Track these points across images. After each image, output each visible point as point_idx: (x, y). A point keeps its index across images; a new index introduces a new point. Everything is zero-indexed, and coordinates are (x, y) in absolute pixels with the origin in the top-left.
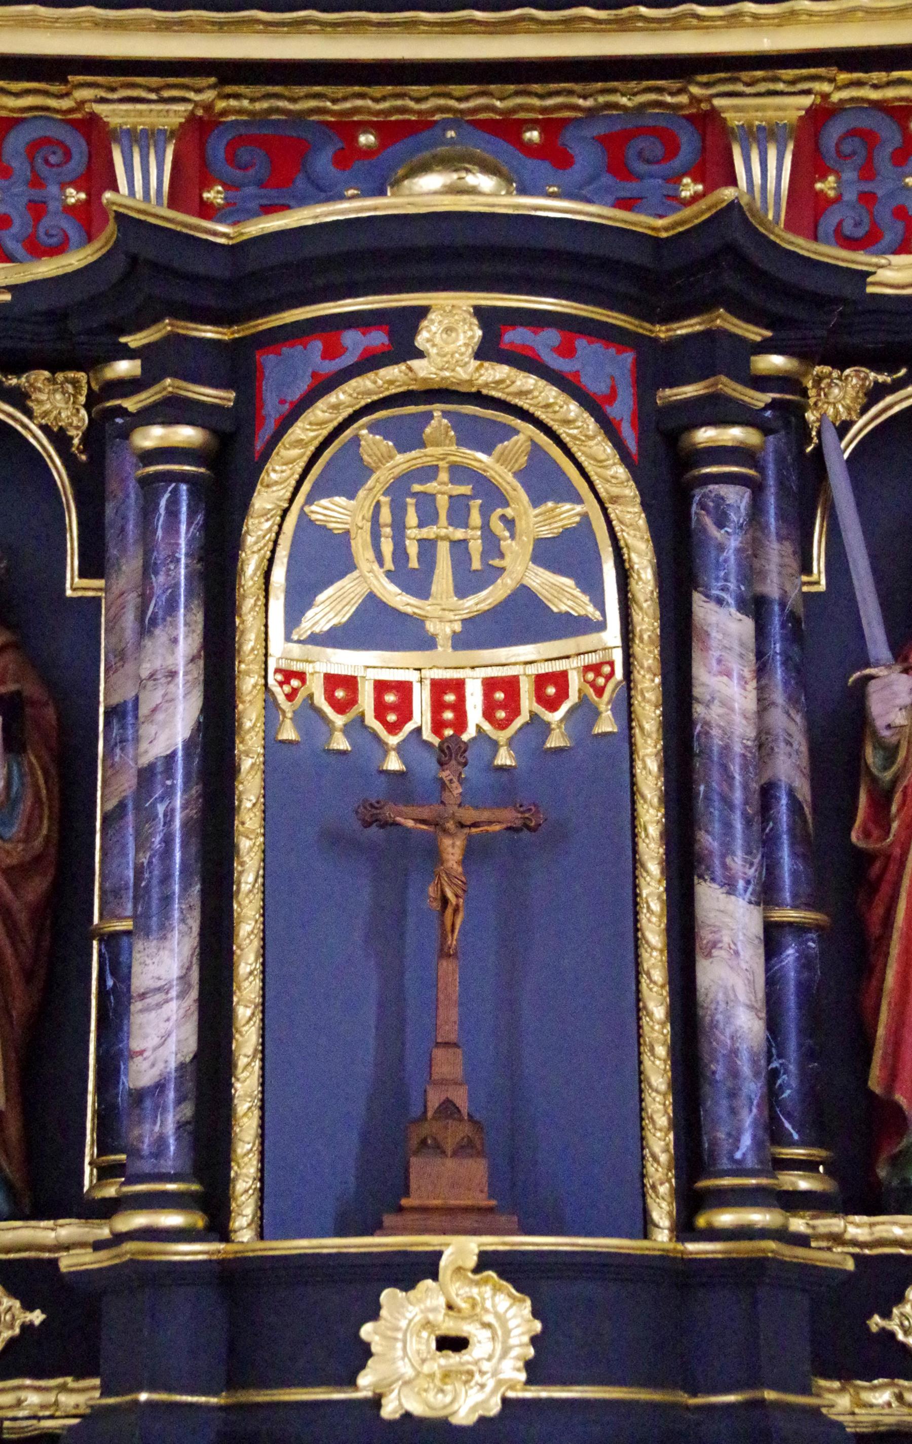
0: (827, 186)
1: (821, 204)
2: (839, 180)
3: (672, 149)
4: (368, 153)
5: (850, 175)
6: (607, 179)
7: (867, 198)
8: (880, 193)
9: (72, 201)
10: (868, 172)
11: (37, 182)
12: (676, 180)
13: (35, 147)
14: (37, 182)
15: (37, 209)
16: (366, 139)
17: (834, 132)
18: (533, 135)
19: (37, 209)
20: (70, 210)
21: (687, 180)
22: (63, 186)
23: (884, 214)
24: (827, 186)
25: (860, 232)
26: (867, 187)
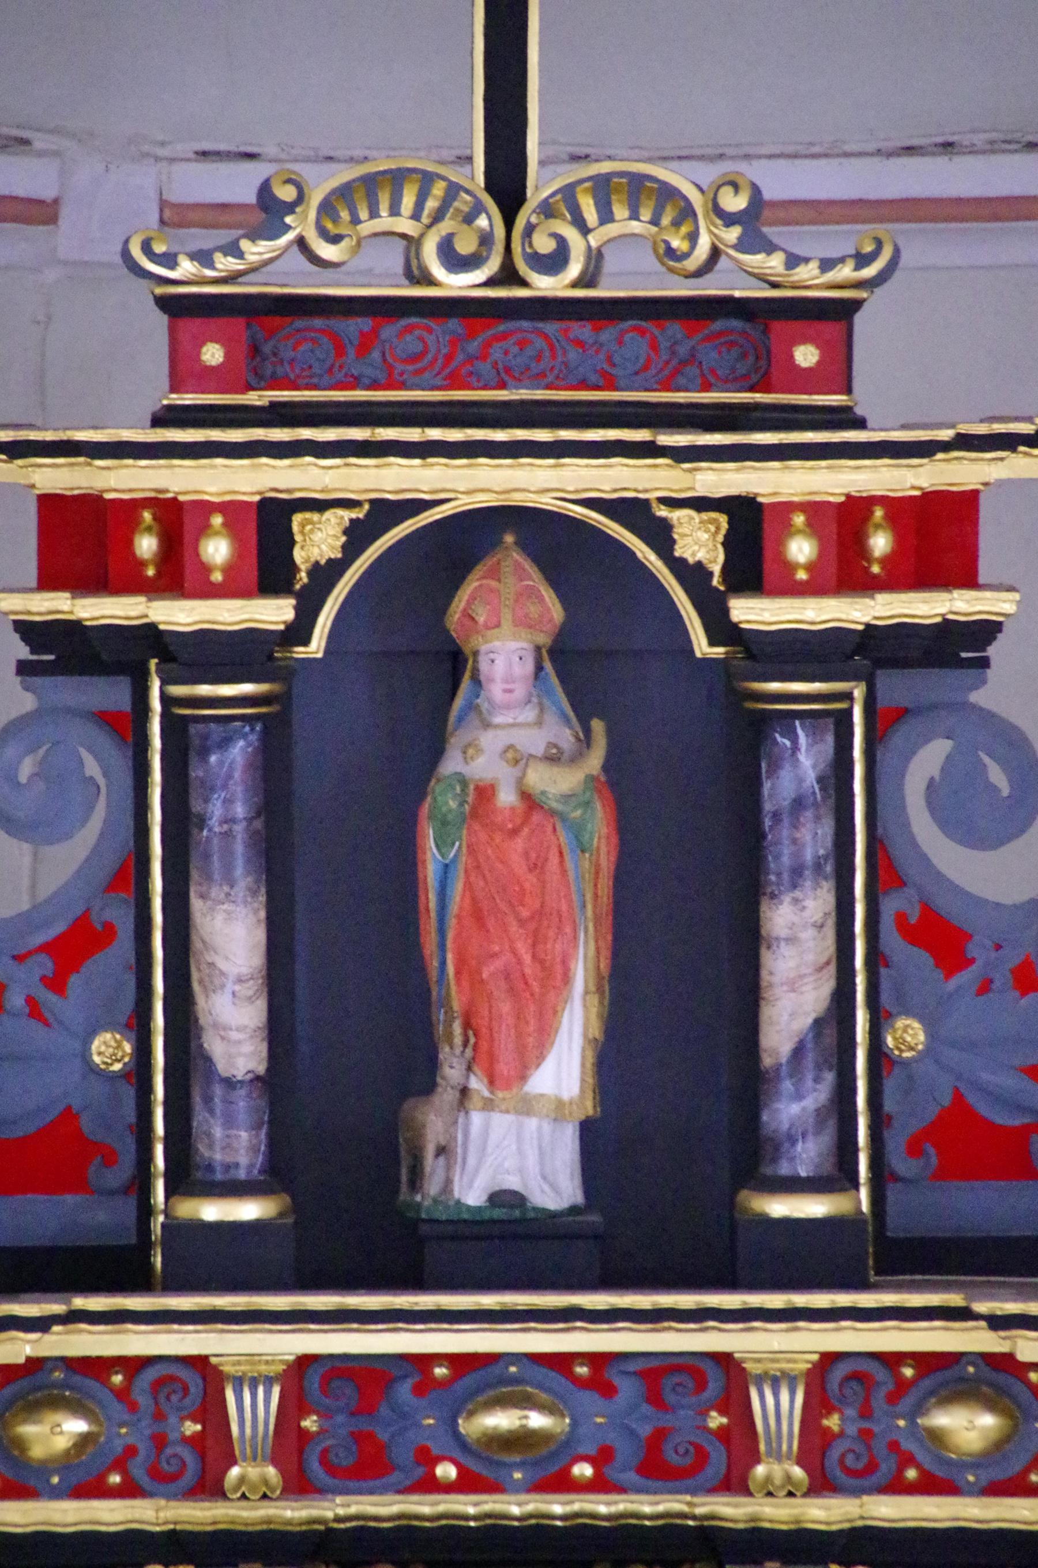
0: (833, 1422)
1: (828, 1438)
2: (842, 1419)
3: (701, 1385)
4: (443, 1384)
5: (851, 1412)
6: (646, 1409)
7: (866, 1435)
8: (876, 1429)
9: (188, 1433)
10: (866, 1412)
11: (159, 1416)
12: (704, 1413)
13: (158, 1385)
14: (159, 1416)
15: (159, 1441)
16: (440, 1371)
17: (840, 1371)
18: (582, 1370)
19: (159, 1441)
20: (187, 1441)
21: (714, 1414)
22: (183, 1419)
23: (880, 1447)
24: (833, 1422)
25: (860, 1466)
26: (866, 1425)
